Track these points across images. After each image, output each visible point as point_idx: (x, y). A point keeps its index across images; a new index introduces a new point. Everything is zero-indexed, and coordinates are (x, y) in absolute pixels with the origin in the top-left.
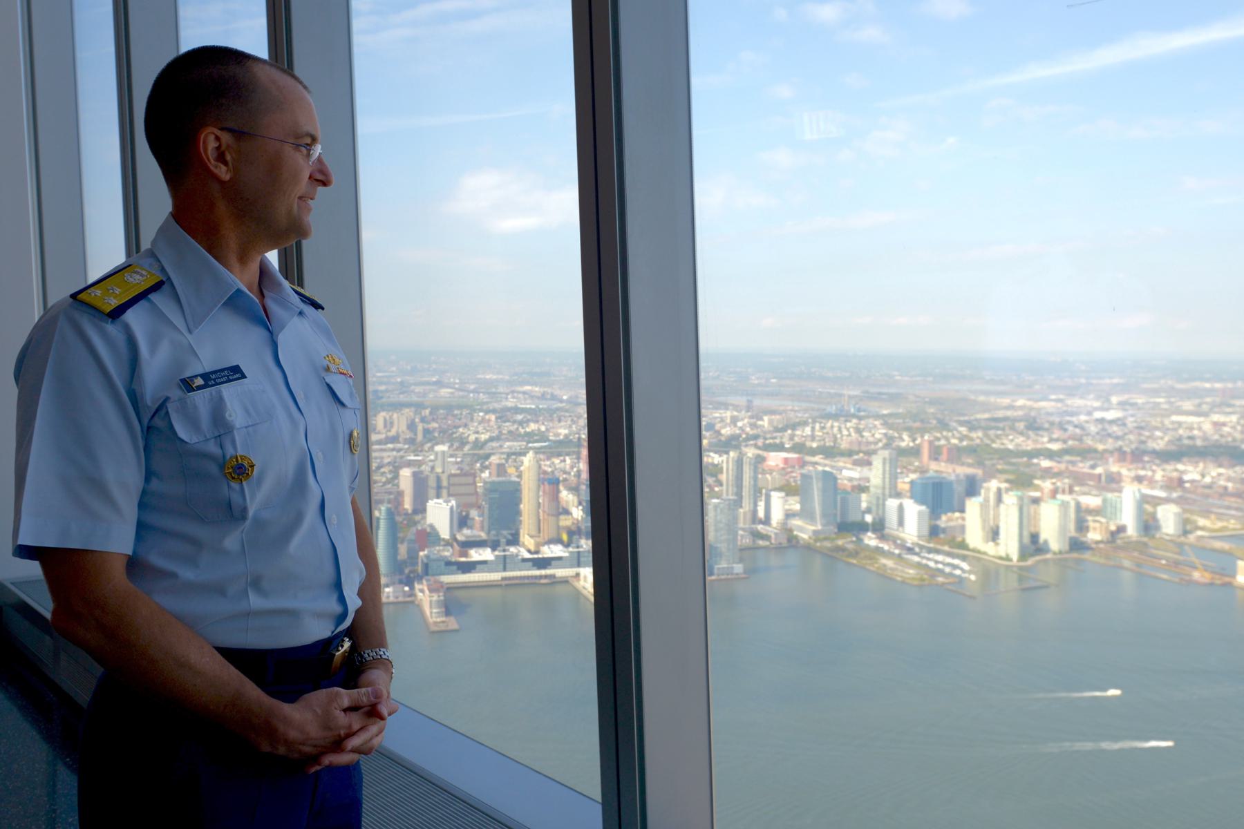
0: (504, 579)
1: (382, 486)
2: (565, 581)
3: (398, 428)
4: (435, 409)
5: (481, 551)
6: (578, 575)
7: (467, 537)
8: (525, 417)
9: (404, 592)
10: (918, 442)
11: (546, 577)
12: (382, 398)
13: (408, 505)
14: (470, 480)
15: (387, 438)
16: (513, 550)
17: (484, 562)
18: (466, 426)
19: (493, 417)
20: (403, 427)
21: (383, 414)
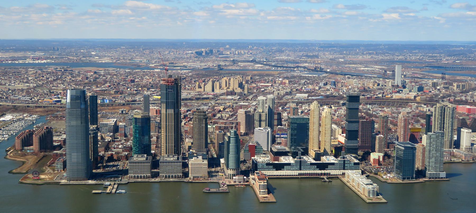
0: (300, 174)
2: (336, 177)
5: (287, 157)
6: (344, 174)
9: (244, 179)
13: (242, 130)
15: (227, 92)
17: (289, 164)
19: (287, 81)
20: (237, 85)
21: (225, 78)
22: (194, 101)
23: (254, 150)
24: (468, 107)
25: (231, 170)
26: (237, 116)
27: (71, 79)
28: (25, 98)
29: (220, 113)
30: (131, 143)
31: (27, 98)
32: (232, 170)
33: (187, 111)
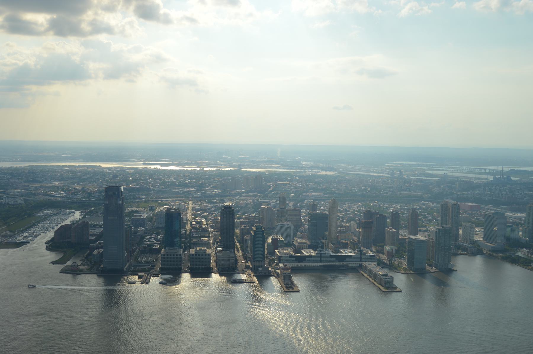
0: (320, 266)
17: (310, 257)
24: (470, 204)
25: (256, 262)
30: (161, 237)
32: (257, 261)
33: (212, 207)
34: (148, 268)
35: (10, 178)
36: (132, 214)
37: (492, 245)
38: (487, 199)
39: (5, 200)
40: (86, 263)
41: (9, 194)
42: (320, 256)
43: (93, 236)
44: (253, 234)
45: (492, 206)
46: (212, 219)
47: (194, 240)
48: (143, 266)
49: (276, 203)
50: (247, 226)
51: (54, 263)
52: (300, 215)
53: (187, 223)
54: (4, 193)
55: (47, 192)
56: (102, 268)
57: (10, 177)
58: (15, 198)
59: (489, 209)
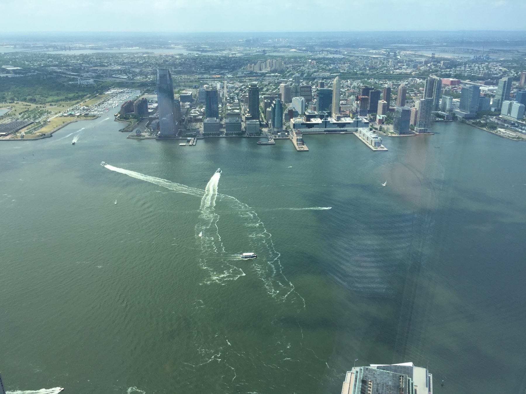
0: (325, 131)
1: (271, 91)
3: (276, 67)
4: (290, 58)
5: (316, 119)
6: (357, 131)
7: (309, 113)
8: (329, 62)
10: (520, 73)
11: (343, 131)
12: (266, 53)
14: (309, 89)
15: (271, 71)
16: (329, 119)
18: (303, 66)
22: (247, 78)
23: (292, 114)
24: (451, 79)
26: (279, 89)
27: (155, 62)
28: (124, 77)
29: (266, 87)
30: (203, 110)
31: (126, 77)
33: (242, 86)
34: (194, 134)
35: (82, 63)
36: (180, 92)
37: (466, 113)
38: (466, 75)
39: (80, 81)
40: (147, 131)
41: (83, 77)
42: (326, 124)
43: (151, 110)
44: (273, 107)
45: (470, 81)
46: (242, 95)
47: (228, 112)
48: (190, 132)
49: (292, 82)
50: (269, 100)
51: (122, 131)
52: (311, 91)
53: (223, 98)
54: (78, 75)
55: (112, 75)
56: (159, 134)
57: (82, 63)
58: (87, 79)
59: (466, 84)
